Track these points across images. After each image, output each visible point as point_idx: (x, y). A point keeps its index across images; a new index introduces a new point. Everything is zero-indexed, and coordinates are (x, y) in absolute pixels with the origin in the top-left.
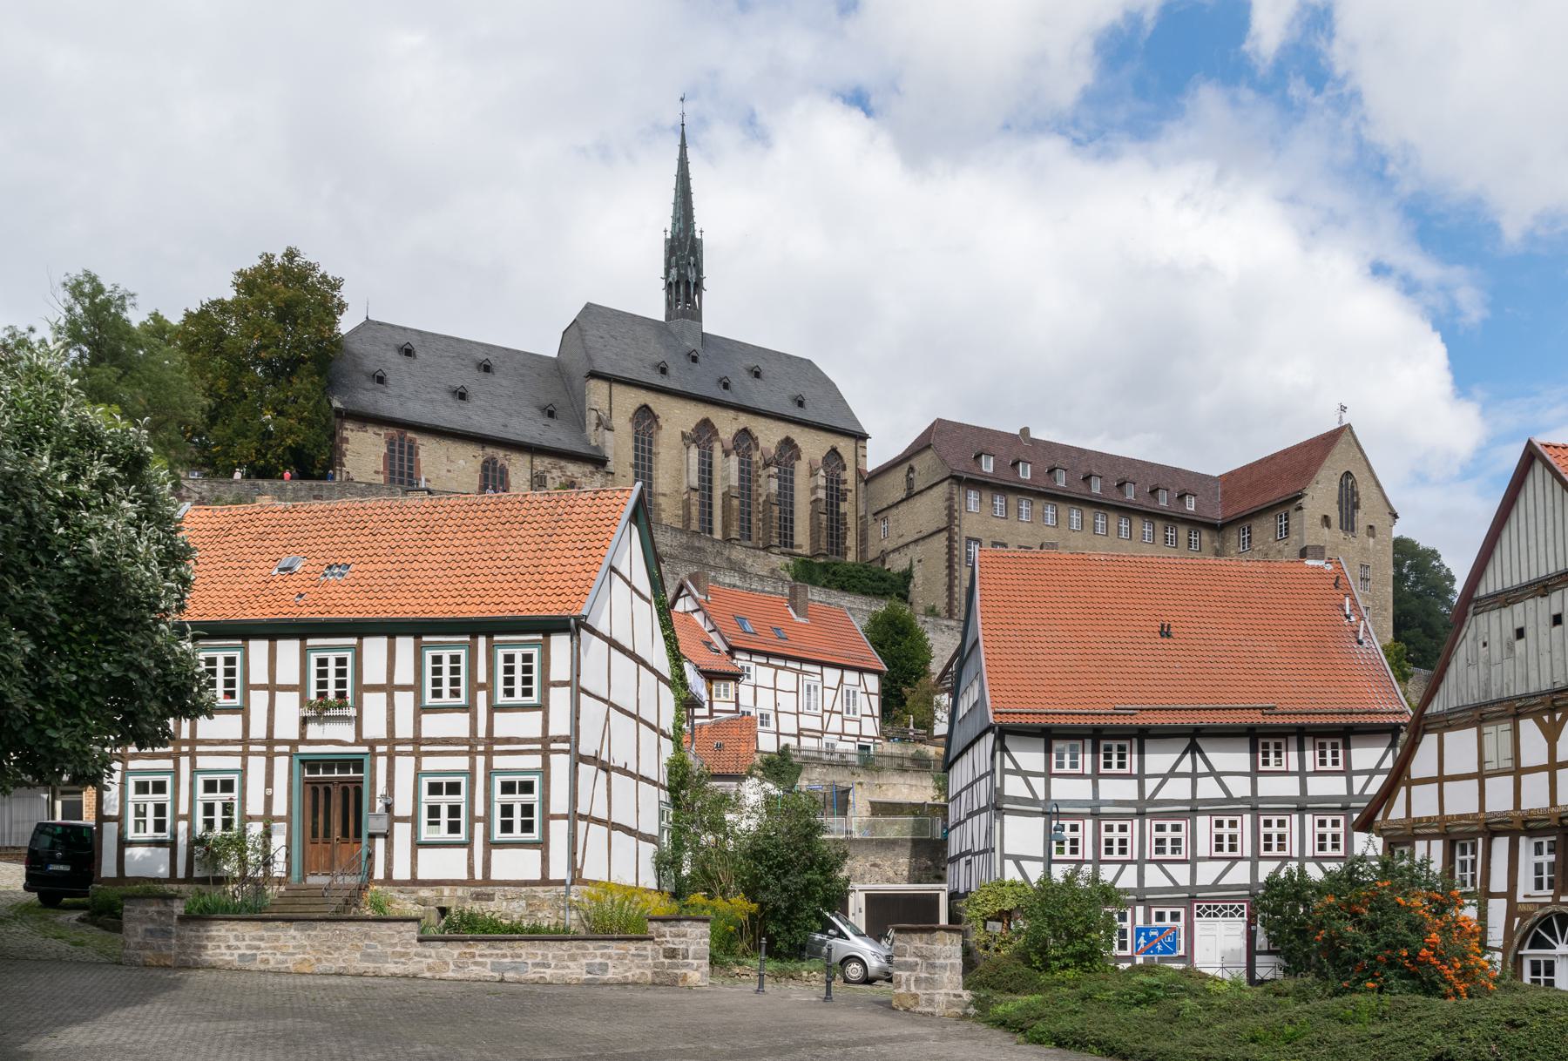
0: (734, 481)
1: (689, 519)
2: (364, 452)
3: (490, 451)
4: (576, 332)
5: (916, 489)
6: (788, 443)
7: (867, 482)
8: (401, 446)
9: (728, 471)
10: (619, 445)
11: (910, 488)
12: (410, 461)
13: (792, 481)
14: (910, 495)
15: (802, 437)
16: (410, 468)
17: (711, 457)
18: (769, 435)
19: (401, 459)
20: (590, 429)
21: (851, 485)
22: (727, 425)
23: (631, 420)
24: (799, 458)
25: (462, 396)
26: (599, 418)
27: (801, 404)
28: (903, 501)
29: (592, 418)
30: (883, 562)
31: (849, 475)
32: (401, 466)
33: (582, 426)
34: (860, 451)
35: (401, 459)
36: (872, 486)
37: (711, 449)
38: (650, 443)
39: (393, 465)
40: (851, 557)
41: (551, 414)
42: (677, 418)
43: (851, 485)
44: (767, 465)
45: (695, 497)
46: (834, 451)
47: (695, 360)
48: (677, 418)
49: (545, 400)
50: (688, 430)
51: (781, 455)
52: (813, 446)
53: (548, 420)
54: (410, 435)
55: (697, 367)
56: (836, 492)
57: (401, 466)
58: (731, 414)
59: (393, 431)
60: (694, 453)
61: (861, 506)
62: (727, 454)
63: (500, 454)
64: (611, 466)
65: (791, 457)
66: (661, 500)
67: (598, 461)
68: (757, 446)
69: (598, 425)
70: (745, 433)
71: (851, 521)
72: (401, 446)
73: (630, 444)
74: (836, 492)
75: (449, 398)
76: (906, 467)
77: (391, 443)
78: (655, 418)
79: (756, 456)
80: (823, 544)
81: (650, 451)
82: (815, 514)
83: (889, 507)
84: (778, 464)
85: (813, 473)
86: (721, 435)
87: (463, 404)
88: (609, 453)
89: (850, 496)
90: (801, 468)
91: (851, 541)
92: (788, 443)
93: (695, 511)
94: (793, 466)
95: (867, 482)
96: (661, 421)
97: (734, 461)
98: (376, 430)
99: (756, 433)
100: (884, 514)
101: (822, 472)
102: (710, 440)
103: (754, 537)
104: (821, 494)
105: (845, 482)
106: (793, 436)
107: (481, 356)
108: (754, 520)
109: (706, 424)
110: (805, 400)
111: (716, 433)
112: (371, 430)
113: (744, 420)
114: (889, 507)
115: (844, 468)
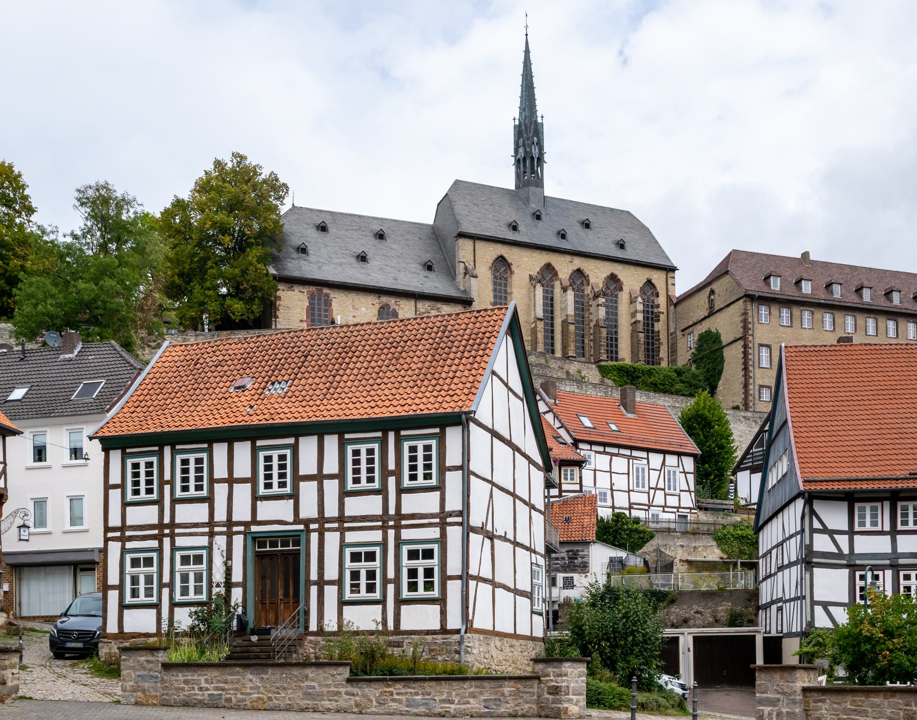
2: (293, 307)
3: (384, 299)
4: (445, 205)
6: (613, 278)
8: (319, 299)
11: (711, 307)
13: (616, 308)
15: (623, 273)
17: (552, 292)
18: (598, 273)
20: (460, 277)
22: (565, 267)
23: (490, 268)
24: (621, 289)
25: (363, 258)
26: (466, 268)
28: (705, 318)
29: (461, 268)
33: (451, 273)
34: (670, 281)
36: (679, 308)
37: (553, 287)
38: (506, 285)
41: (430, 268)
42: (526, 264)
43: (663, 308)
44: (596, 296)
46: (649, 282)
48: (526, 264)
49: (426, 257)
50: (534, 273)
51: (608, 288)
52: (632, 279)
53: (428, 273)
54: (326, 291)
58: (568, 258)
59: (313, 289)
60: (539, 291)
62: (565, 290)
63: (392, 301)
68: (588, 282)
69: (465, 274)
70: (579, 272)
72: (319, 299)
73: (490, 287)
75: (353, 260)
77: (311, 298)
78: (509, 265)
81: (506, 292)
83: (695, 324)
84: (605, 295)
85: (632, 301)
86: (560, 276)
87: (362, 264)
88: (474, 295)
90: (624, 297)
92: (613, 278)
94: (617, 296)
96: (513, 268)
97: (570, 294)
98: (301, 288)
99: (587, 272)
100: (691, 329)
101: (640, 299)
102: (551, 280)
106: (616, 273)
107: (377, 228)
110: (627, 245)
112: (297, 288)
113: (578, 263)
114: (695, 324)
115: (657, 295)
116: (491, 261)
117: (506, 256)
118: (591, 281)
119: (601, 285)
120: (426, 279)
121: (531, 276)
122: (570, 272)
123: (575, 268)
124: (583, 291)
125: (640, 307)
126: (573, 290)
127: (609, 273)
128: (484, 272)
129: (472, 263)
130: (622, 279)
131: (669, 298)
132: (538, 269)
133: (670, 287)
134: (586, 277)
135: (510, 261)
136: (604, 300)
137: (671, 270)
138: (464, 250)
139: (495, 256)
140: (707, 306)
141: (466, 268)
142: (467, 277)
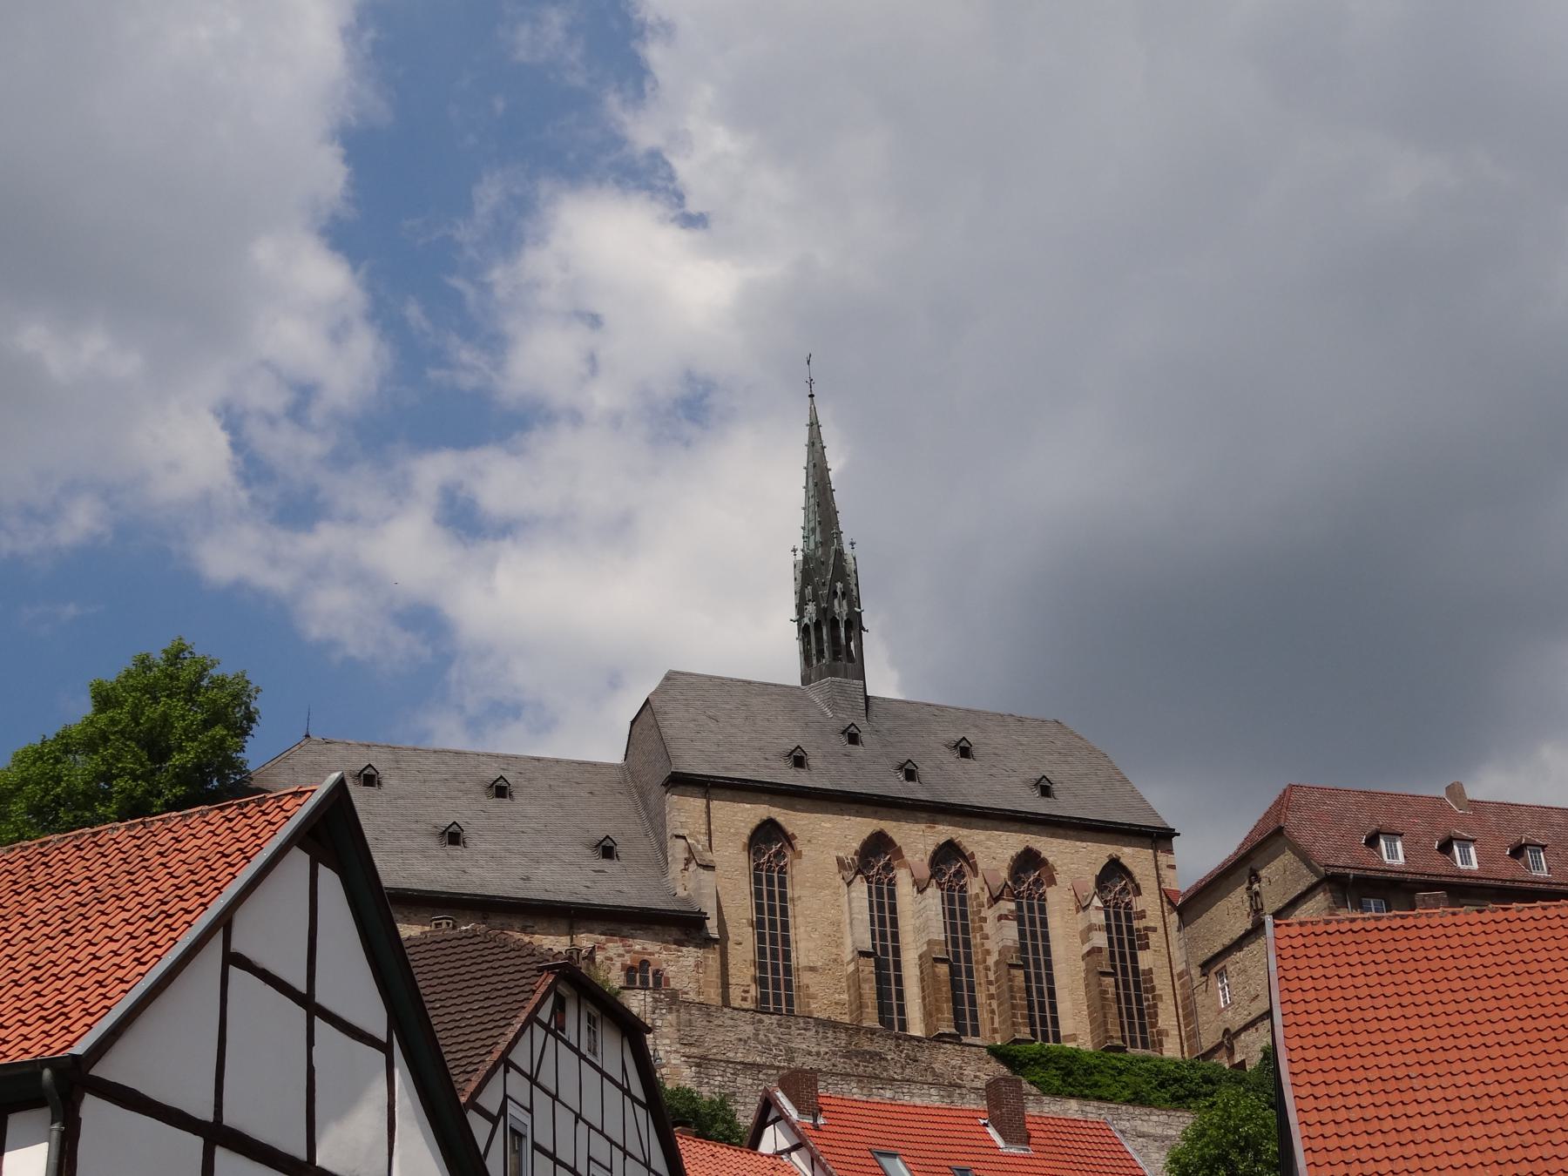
0: (938, 932)
1: (861, 1007)
9: (921, 917)
10: (726, 890)
15: (1051, 848)
18: (994, 851)
22: (917, 841)
26: (690, 849)
27: (1046, 791)
29: (678, 850)
31: (1148, 903)
37: (892, 883)
40: (1172, 1049)
42: (825, 839)
43: (1153, 918)
44: (995, 899)
45: (868, 966)
47: (854, 739)
48: (825, 839)
52: (1077, 862)
55: (857, 750)
56: (1125, 937)
60: (861, 889)
64: (712, 927)
65: (1038, 882)
66: (806, 978)
67: (686, 926)
68: (974, 869)
69: (688, 862)
71: (1162, 983)
73: (745, 886)
74: (1125, 937)
78: (789, 839)
79: (974, 886)
80: (1115, 1031)
82: (1095, 974)
86: (908, 856)
90: (1057, 900)
91: (1167, 1018)
92: (1028, 861)
93: (869, 991)
94: (1042, 898)
97: (934, 896)
101: (1097, 902)
102: (888, 867)
103: (985, 1028)
104: (1100, 939)
105: (1142, 915)
108: (981, 998)
109: (878, 846)
111: (898, 853)
116: (748, 832)
117: (780, 819)
118: (981, 866)
119: (1004, 874)
120: (599, 877)
121: (840, 861)
122: (931, 849)
123: (942, 840)
124: (962, 889)
125: (1099, 918)
126: (940, 885)
127: (1020, 849)
128: (732, 858)
129: (703, 839)
130: (1050, 860)
131: (1167, 897)
132: (856, 845)
133: (1164, 872)
134: (969, 859)
135: (790, 830)
136: (1012, 906)
137: (1159, 838)
138: (686, 811)
139: (757, 822)
141: (690, 849)
142: (693, 866)
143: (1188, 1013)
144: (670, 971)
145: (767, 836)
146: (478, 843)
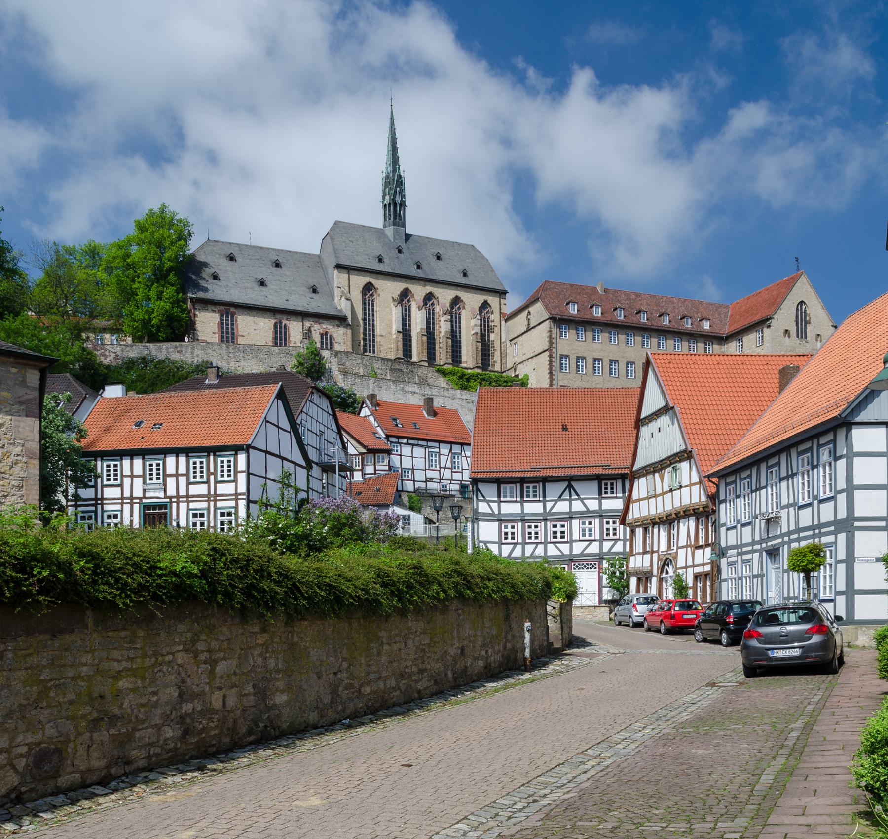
2: (207, 323)
5: (532, 326)
7: (506, 321)
12: (232, 325)
14: (528, 330)
15: (464, 296)
16: (233, 329)
18: (445, 296)
19: (227, 324)
21: (497, 323)
25: (262, 284)
26: (342, 292)
30: (515, 370)
31: (495, 317)
32: (228, 329)
35: (227, 324)
39: (222, 328)
54: (232, 309)
57: (228, 329)
59: (222, 308)
61: (503, 336)
75: (255, 285)
76: (526, 311)
79: (437, 309)
83: (518, 337)
87: (263, 289)
89: (496, 330)
92: (456, 301)
95: (506, 321)
98: (213, 308)
112: (210, 307)
113: (429, 289)
114: (518, 337)
115: (492, 313)
123: (428, 292)
140: (526, 323)
141: (342, 292)
143: (503, 356)
144: (335, 335)
145: (368, 288)
146: (271, 286)
